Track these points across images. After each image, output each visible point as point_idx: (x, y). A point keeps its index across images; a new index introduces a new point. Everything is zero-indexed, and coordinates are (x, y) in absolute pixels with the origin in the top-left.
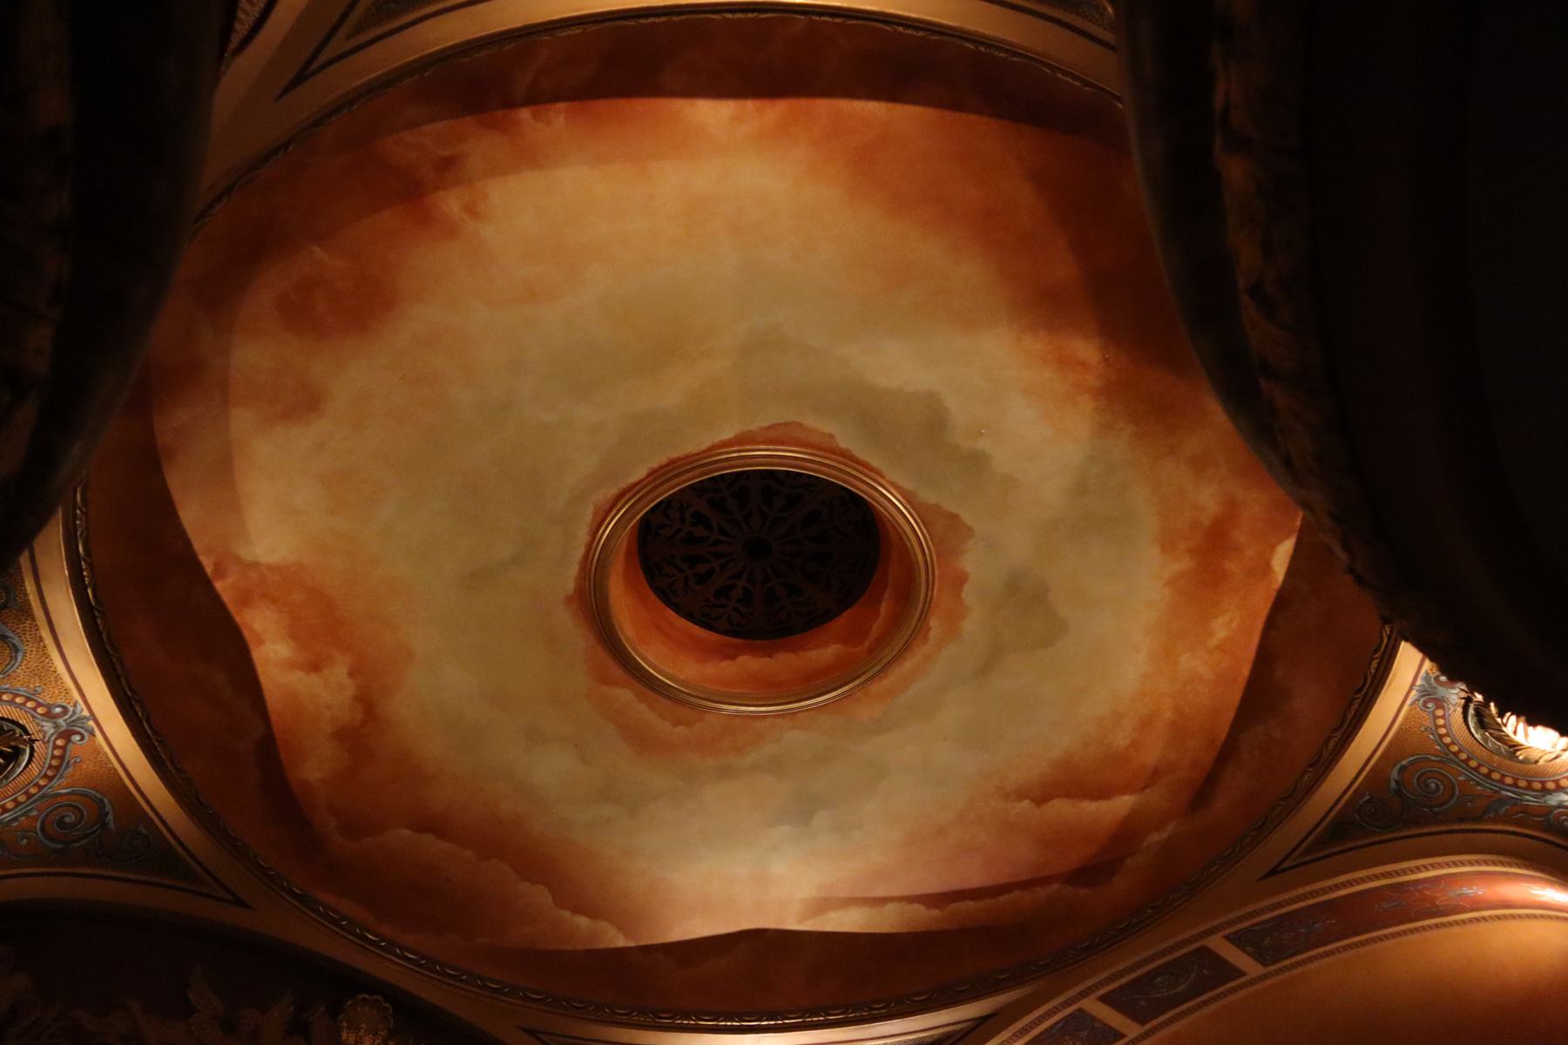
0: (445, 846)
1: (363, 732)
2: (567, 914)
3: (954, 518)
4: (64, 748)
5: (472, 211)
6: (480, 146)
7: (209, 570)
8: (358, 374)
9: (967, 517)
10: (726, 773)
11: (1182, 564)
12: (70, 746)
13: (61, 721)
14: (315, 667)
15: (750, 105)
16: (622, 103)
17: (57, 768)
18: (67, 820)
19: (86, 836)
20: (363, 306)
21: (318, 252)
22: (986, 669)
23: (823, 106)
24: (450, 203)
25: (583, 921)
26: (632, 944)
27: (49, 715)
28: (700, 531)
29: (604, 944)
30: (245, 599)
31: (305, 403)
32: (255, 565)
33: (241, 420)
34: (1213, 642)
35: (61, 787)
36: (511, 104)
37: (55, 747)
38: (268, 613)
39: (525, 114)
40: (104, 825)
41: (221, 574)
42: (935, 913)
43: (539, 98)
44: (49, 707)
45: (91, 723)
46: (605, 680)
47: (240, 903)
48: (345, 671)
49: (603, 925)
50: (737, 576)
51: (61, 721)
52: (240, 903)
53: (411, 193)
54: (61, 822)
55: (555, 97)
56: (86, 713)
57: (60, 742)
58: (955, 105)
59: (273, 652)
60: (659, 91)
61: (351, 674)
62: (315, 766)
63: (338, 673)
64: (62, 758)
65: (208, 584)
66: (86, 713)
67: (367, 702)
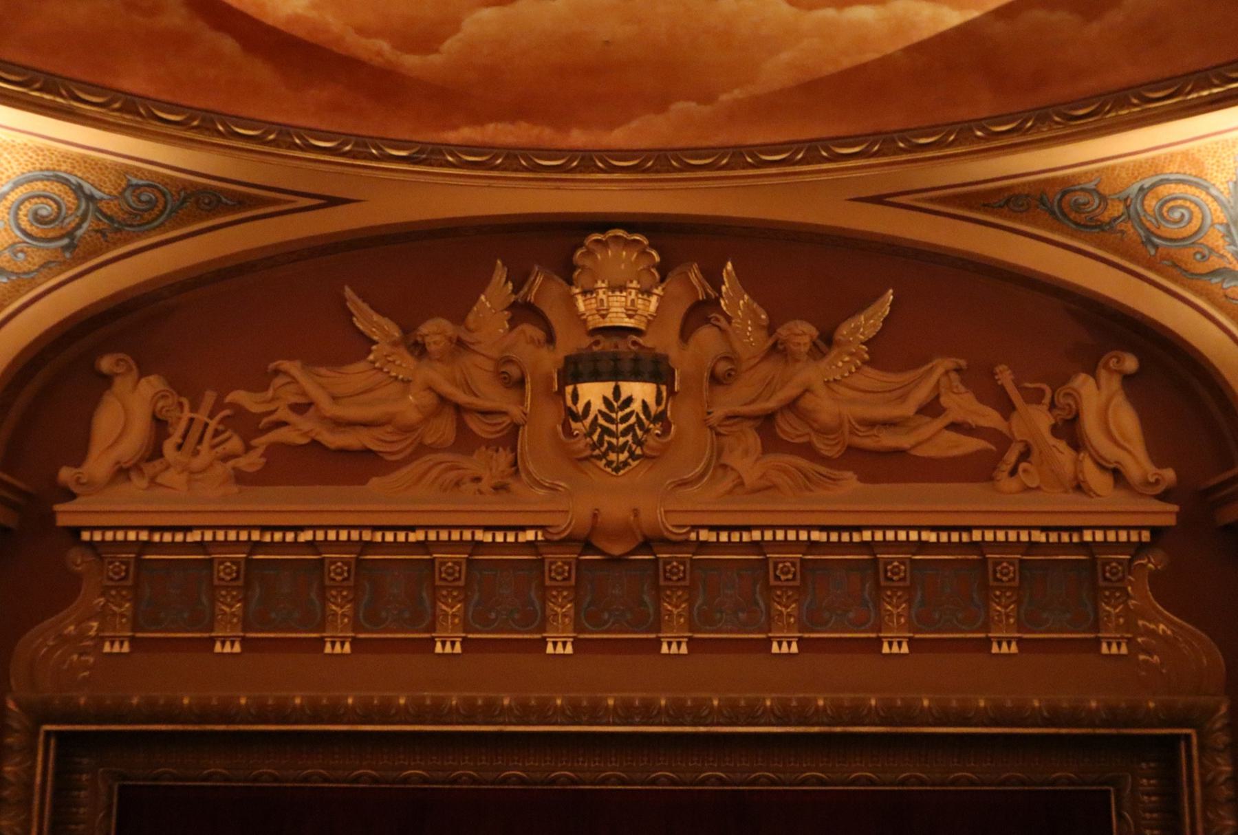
18: (44, 212)
40: (90, 198)
54: (38, 219)
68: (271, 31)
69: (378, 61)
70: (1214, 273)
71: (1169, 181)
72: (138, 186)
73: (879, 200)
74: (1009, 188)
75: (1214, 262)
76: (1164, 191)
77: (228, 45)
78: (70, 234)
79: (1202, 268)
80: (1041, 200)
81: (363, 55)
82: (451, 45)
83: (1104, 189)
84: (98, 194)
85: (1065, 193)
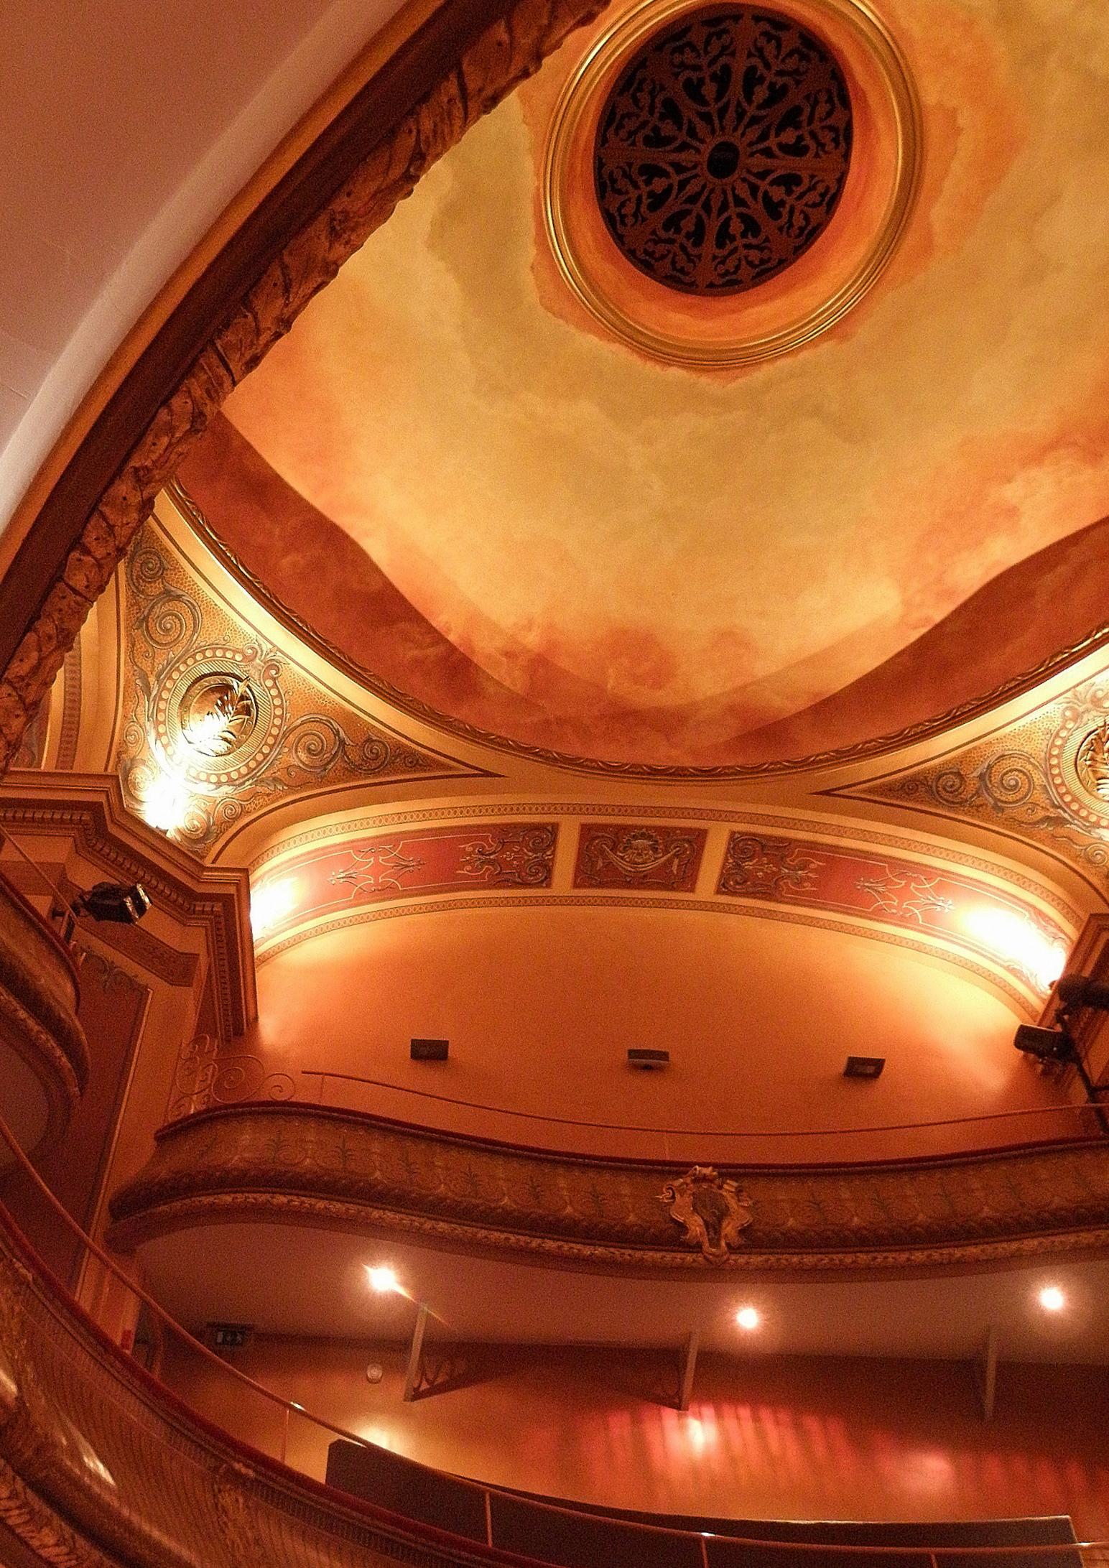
5: (529, 626)
6: (485, 647)
7: (924, 630)
8: (687, 623)
14: (1012, 513)
15: (353, 535)
16: (407, 596)
23: (318, 503)
24: (532, 640)
27: (1077, 717)
28: (736, 227)
30: (950, 593)
32: (907, 604)
33: (762, 668)
36: (452, 648)
39: (452, 638)
43: (438, 637)
44: (1065, 720)
45: (1079, 689)
46: (928, 247)
48: (1008, 486)
50: (768, 153)
51: (1081, 709)
53: (541, 666)
55: (431, 630)
58: (248, 446)
59: (1005, 551)
60: (388, 585)
63: (1012, 492)
66: (1069, 694)
67: (1038, 453)
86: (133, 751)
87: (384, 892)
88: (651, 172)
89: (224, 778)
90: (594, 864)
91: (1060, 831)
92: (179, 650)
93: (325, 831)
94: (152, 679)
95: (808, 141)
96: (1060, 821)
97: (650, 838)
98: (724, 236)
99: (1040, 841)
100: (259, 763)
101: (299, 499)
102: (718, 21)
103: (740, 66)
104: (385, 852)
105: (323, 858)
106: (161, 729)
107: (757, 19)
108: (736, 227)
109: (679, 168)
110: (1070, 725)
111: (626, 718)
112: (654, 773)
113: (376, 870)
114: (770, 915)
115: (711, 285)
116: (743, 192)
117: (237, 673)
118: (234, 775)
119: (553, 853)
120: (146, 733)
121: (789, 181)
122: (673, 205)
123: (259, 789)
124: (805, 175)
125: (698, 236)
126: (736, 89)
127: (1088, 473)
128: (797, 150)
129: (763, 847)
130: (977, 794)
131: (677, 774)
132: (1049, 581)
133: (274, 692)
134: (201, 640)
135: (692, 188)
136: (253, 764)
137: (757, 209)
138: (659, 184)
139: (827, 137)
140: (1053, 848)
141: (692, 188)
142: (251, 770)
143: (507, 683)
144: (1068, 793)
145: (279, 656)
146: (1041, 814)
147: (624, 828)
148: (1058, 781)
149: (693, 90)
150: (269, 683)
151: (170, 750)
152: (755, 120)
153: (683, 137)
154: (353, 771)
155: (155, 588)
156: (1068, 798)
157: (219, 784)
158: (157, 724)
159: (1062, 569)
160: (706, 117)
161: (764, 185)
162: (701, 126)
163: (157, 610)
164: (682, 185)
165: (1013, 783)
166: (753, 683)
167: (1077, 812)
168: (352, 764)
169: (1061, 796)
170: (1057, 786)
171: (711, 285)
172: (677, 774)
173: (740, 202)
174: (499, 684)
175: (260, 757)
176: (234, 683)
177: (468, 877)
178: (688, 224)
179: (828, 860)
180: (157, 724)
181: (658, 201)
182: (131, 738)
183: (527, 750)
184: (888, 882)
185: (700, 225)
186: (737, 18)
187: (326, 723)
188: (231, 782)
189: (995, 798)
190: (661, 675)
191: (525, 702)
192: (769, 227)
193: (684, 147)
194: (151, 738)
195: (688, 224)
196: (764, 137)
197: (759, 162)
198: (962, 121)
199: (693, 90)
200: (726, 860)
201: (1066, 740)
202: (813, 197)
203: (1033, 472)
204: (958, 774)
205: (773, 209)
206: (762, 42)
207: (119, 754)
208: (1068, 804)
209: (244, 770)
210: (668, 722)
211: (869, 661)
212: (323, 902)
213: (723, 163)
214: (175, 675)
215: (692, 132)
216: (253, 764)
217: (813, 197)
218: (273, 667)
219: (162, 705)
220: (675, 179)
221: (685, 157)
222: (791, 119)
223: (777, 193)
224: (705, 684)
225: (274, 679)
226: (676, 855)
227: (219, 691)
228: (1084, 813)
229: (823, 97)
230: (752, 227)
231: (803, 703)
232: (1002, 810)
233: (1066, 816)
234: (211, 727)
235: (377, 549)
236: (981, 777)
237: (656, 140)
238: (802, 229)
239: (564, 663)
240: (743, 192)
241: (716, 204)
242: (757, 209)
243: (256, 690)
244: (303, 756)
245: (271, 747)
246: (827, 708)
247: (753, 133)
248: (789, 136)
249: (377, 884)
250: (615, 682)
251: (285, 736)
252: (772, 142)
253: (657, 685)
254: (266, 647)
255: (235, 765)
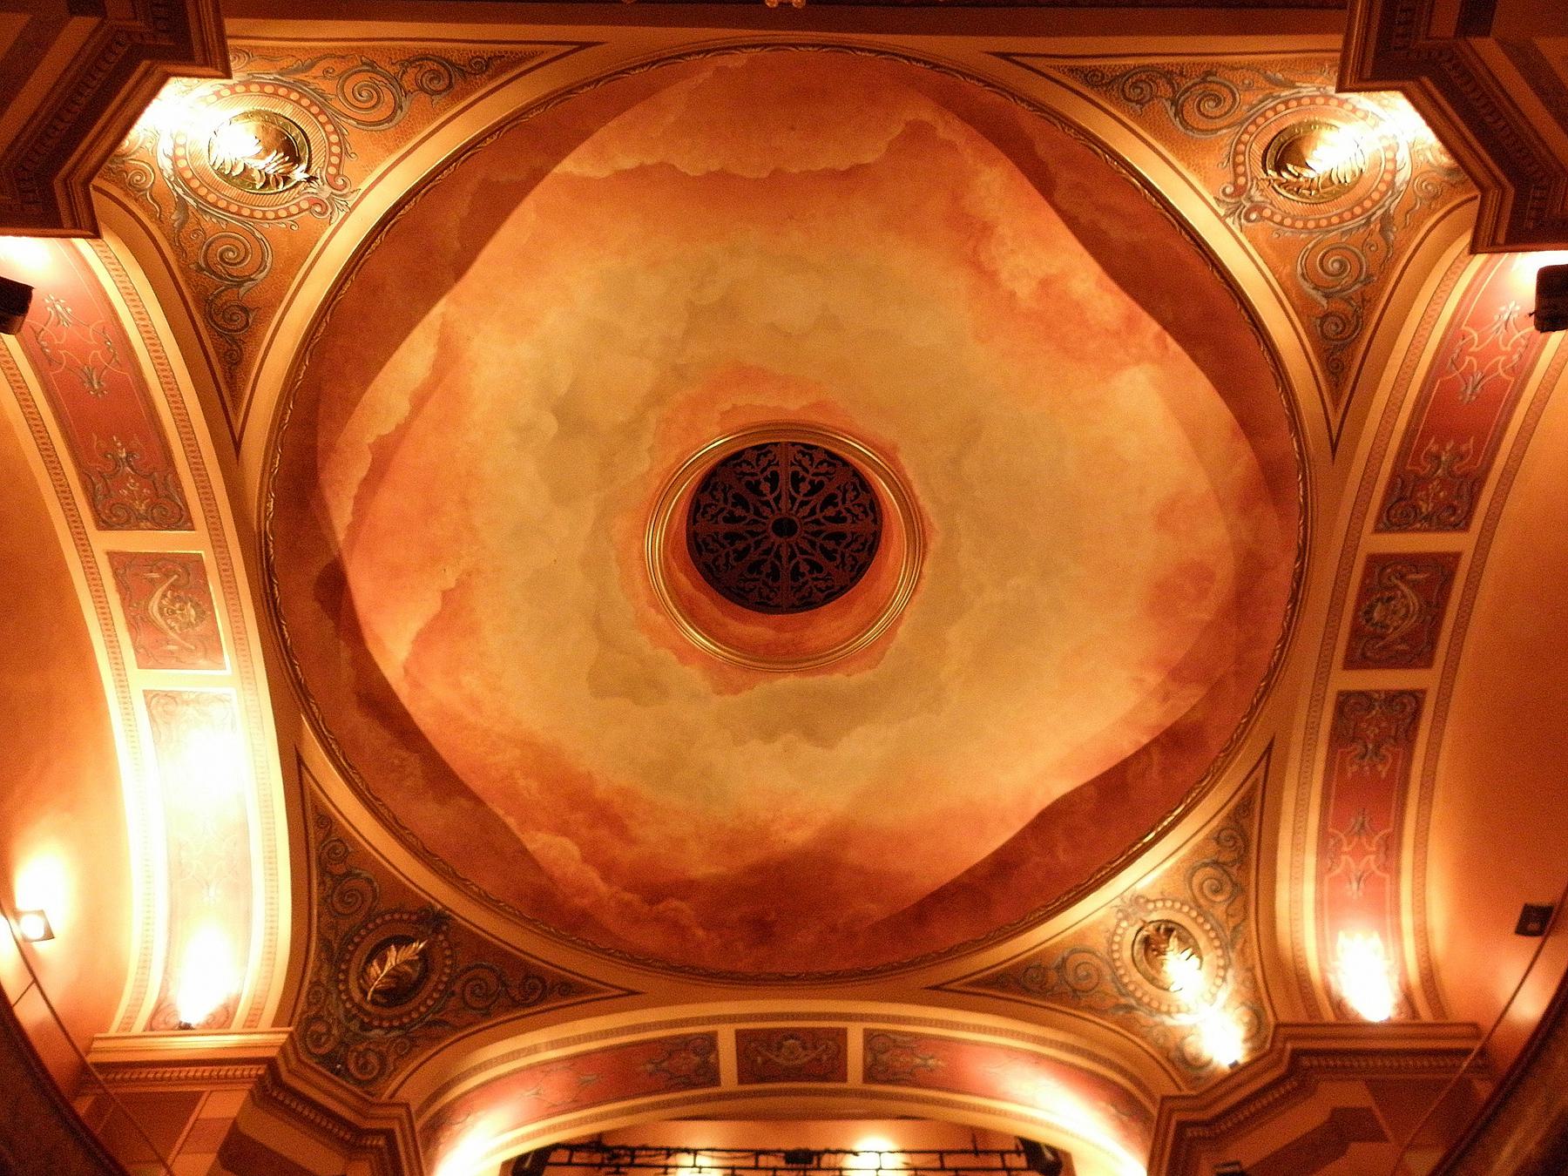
0: (822, 164)
1: (970, 235)
2: (649, 161)
3: (737, 691)
4: (1236, 176)
6: (1157, 717)
7: (1169, 340)
8: (1148, 553)
9: (730, 698)
10: (657, 397)
11: (601, 791)
12: (1230, 177)
13: (1248, 205)
14: (1045, 284)
15: (1047, 802)
17: (1236, 153)
18: (1212, 103)
19: (1189, 89)
20: (1164, 598)
21: (1206, 617)
22: (597, 624)
23: (1018, 826)
24: (1153, 679)
25: (628, 163)
26: (557, 170)
27: (1258, 207)
28: (830, 511)
29: (583, 149)
30: (1130, 322)
31: (1167, 516)
32: (1138, 361)
33: (1200, 484)
34: (518, 774)
35: (1226, 136)
36: (1155, 741)
37: (1245, 174)
38: (1107, 317)
39: (1145, 740)
40: (1174, 103)
41: (1158, 337)
42: (370, 439)
43: (1144, 751)
44: (1261, 218)
45: (1222, 212)
47: (1005, 56)
49: (605, 173)
51: (1248, 205)
52: (1005, 56)
53: (1177, 674)
54: (1218, 101)
55: (1137, 755)
56: (1229, 221)
57: (1242, 180)
58: (969, 872)
59: (1085, 279)
61: (1012, 294)
62: (995, 185)
63: (1024, 290)
64: (1235, 165)
65: (1166, 326)
66: (1229, 221)
67: (985, 275)
68: (1010, 155)
69: (949, 116)
70: (312, 66)
71: (389, 119)
72: (1138, 102)
73: (583, 46)
74: (491, 78)
75: (317, 71)
76: (383, 112)
77: (1041, 149)
78: (1204, 80)
79: (323, 64)
80: (464, 74)
81: (957, 123)
82: (897, 130)
83: (423, 97)
84: (1168, 104)
85: (450, 86)
86: (1171, 1044)
87: (1391, 846)
88: (796, 573)
89: (1221, 973)
90: (1404, 653)
91: (1399, 219)
92: (1106, 971)
93: (1296, 903)
94: (1123, 1001)
95: (768, 473)
96: (1386, 220)
97: (1372, 607)
98: (838, 519)
99: (1410, 240)
100: (1217, 937)
101: (1014, 839)
102: (698, 546)
103: (724, 528)
104: (1339, 843)
105: (1330, 908)
106: (1164, 1008)
107: (695, 522)
108: (830, 511)
109: (792, 556)
110: (1267, 213)
111: (1243, 602)
112: (1296, 599)
113: (1358, 853)
114: (1509, 476)
115: (875, 521)
116: (806, 510)
117: (1137, 928)
118: (1221, 962)
119: (1378, 692)
120: (1162, 1024)
121: (796, 480)
122: (819, 558)
123: (1238, 947)
124: (790, 470)
125: (838, 537)
126: (739, 527)
127: (1004, 230)
128: (774, 480)
129: (1400, 499)
130: (1348, 301)
131: (1300, 579)
132: (1117, 232)
133: (1159, 904)
134: (1102, 949)
135: (806, 546)
136: (1217, 943)
137: (817, 500)
138: (804, 568)
139: (764, 462)
140: (1418, 229)
141: (806, 546)
142: (1220, 947)
143: (1194, 701)
144: (1351, 210)
145: (1128, 894)
146: (1377, 237)
147: (1356, 632)
148: (1335, 220)
149: (741, 555)
150: (1151, 906)
151: (1183, 1008)
152: (757, 512)
153: (771, 558)
154: (1242, 861)
155: (1053, 977)
156: (1358, 210)
157: (1224, 979)
158: (1158, 1011)
159: (1104, 224)
160: (758, 544)
161: (800, 498)
162: (764, 547)
163: (1071, 979)
164: (803, 552)
165: (1336, 265)
166: (1216, 492)
167: (1375, 203)
168: (1240, 860)
169: (1354, 217)
170: (1342, 221)
171: (875, 521)
172: (1300, 579)
173: (813, 512)
174: (1194, 708)
175: (1212, 934)
176: (1144, 933)
177: (1392, 770)
178: (830, 545)
179: (1425, 436)
180: (1158, 1011)
181: (815, 567)
182: (1161, 1041)
183: (1254, 707)
184: (1470, 371)
185: (829, 537)
186: (695, 535)
187: (1194, 870)
188: (1225, 968)
189: (1356, 281)
190: (1199, 574)
191: (1215, 690)
192: (830, 488)
193: (778, 556)
194: (1169, 1021)
195: (830, 545)
196: (767, 504)
197: (784, 504)
198: (727, 406)
199: (741, 555)
200: (1418, 530)
201: (1286, 215)
202: (806, 462)
203: (1004, 275)
204: (1326, 316)
205: (816, 488)
206: (708, 516)
207: (1168, 1059)
208: (1365, 211)
209: (1220, 952)
210: (1251, 568)
211: (1201, 386)
212: (1382, 907)
213: (785, 527)
214: (1126, 980)
215: (767, 552)
216: (1217, 943)
217: (806, 462)
218: (1139, 901)
219: (1146, 999)
220: (799, 557)
221: (784, 553)
222: (754, 488)
223: (805, 487)
224: (1213, 537)
225: (1148, 901)
226: (1402, 577)
227: (1151, 946)
228: (1376, 196)
229: (738, 470)
230: (830, 501)
231: (1244, 447)
232: (1369, 276)
233: (1379, 213)
234: (1178, 966)
235: (1061, 787)
236: (1327, 296)
237: (775, 574)
238: (830, 464)
239: (1180, 653)
240: (806, 510)
241: (815, 528)
242: (817, 500)
243: (1155, 916)
244: (1219, 898)
245: (1206, 921)
246: (1249, 424)
247: (766, 511)
248: (765, 487)
249: (1377, 853)
250: (1204, 613)
251: (1199, 906)
252: (770, 498)
253: (1210, 577)
254: (1118, 902)
255: (1211, 957)
